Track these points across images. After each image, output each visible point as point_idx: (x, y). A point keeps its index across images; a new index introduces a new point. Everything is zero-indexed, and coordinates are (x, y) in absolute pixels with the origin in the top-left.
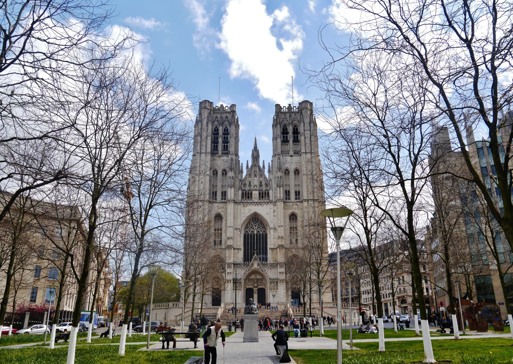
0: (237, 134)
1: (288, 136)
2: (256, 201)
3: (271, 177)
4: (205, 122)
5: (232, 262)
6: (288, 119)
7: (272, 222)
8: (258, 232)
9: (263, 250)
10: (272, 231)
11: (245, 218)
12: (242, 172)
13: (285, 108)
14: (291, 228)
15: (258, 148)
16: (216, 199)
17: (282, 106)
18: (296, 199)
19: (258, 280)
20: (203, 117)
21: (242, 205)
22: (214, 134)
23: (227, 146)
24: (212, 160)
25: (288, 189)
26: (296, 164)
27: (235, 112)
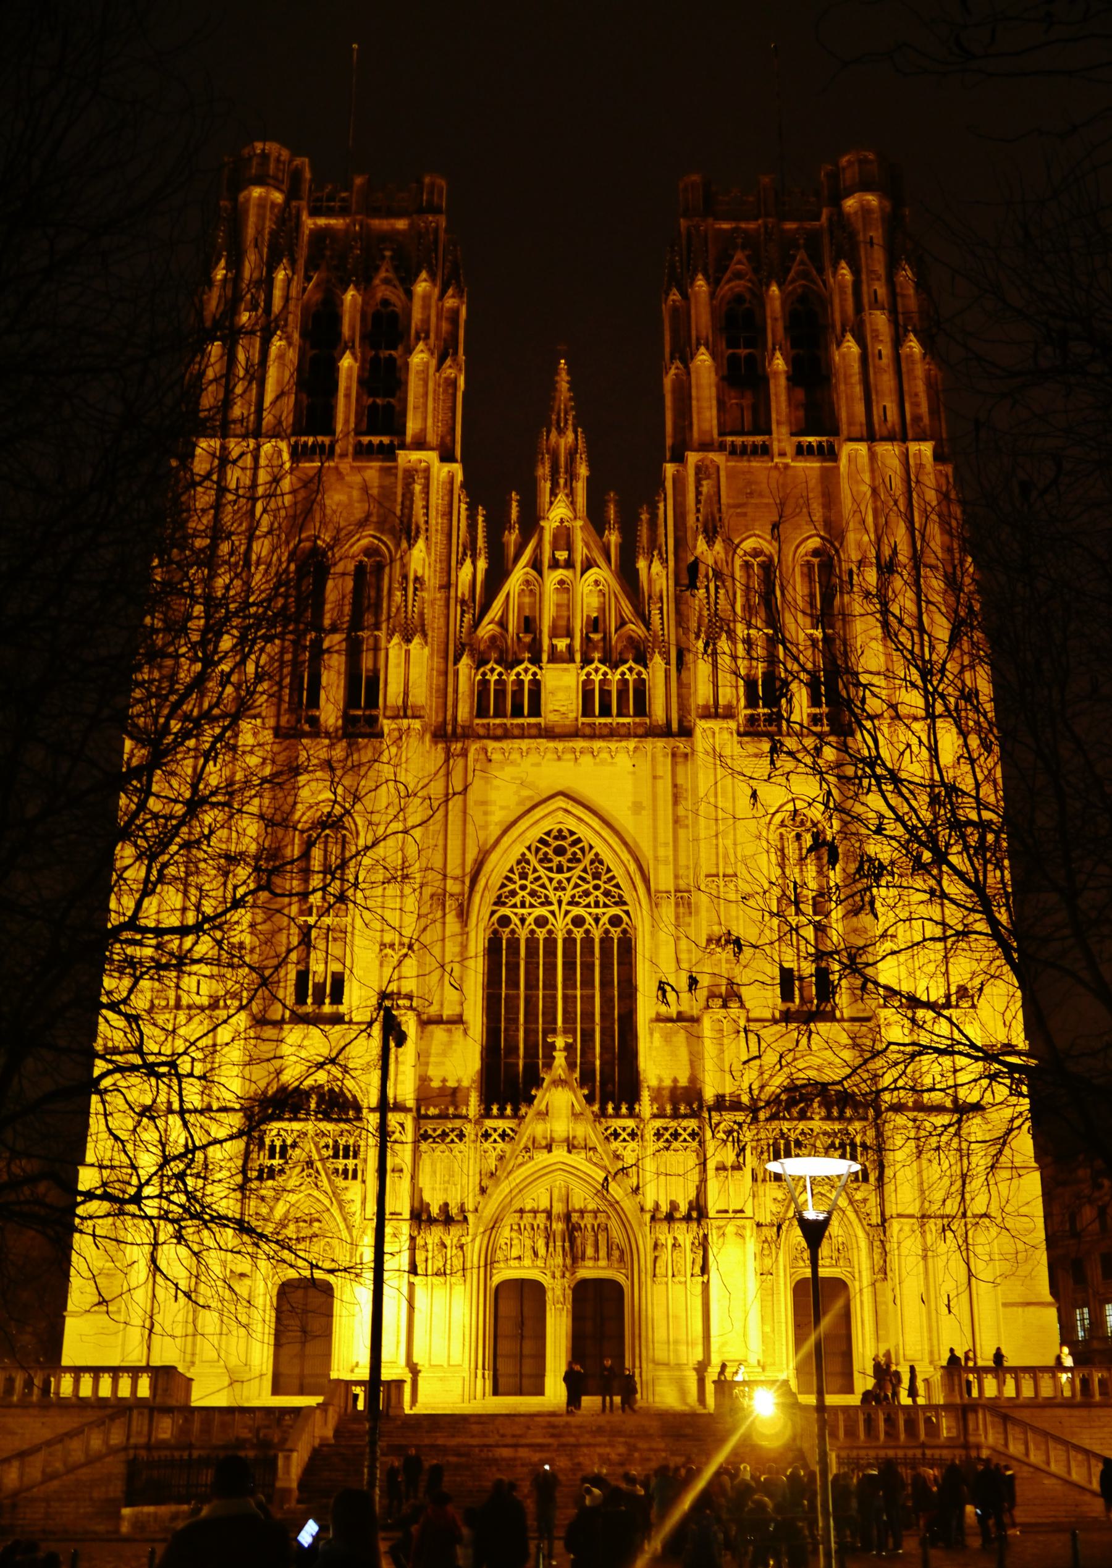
8: (578, 921)
16: (314, 721)
18: (815, 719)
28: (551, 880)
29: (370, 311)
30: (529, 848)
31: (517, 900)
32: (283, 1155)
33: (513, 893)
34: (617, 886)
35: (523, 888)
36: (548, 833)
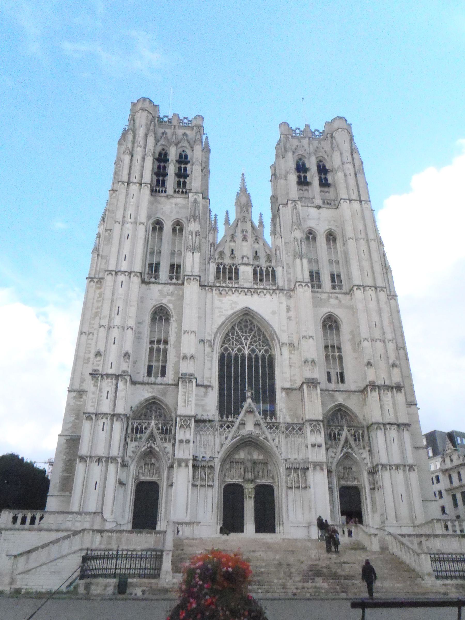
1: (308, 175)
3: (280, 242)
4: (141, 132)
5: (193, 413)
7: (284, 331)
8: (253, 351)
9: (264, 392)
10: (285, 351)
14: (326, 347)
15: (249, 190)
18: (334, 287)
19: (255, 463)
21: (215, 291)
23: (185, 183)
24: (151, 203)
25: (314, 269)
26: (329, 222)
28: (243, 336)
30: (235, 325)
31: (231, 342)
32: (141, 432)
33: (229, 340)
34: (267, 339)
35: (233, 338)
36: (242, 320)
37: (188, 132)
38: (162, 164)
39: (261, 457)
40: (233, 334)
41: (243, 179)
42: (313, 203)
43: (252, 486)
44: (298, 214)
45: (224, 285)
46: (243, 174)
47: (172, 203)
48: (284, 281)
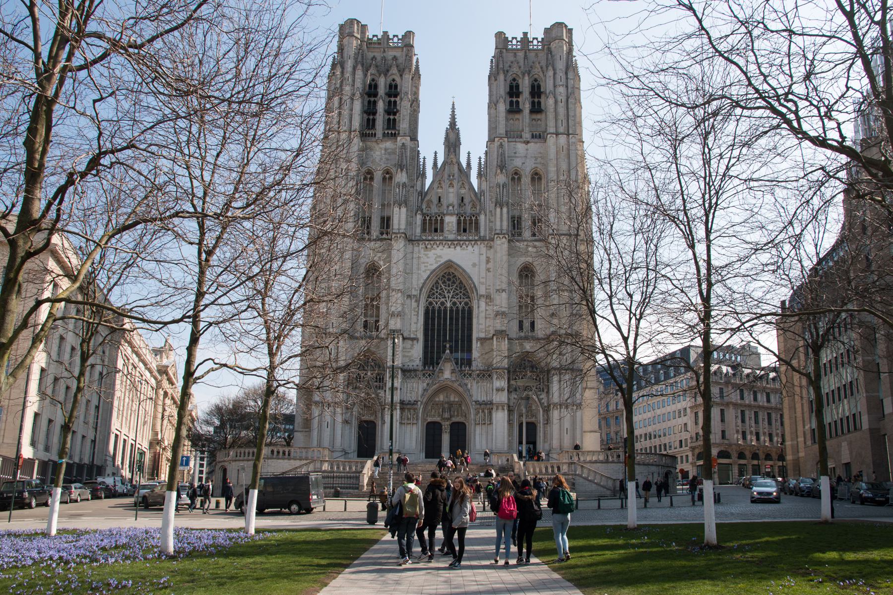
0: (416, 94)
1: (520, 100)
2: (451, 237)
3: (484, 187)
6: (522, 63)
7: (482, 284)
8: (454, 303)
9: (463, 341)
10: (483, 304)
11: (428, 273)
12: (423, 175)
13: (514, 42)
15: (459, 125)
17: (509, 36)
19: (451, 404)
20: (345, 55)
22: (369, 95)
23: (394, 120)
25: (516, 213)
27: (412, 46)
29: (388, 83)
37: (398, 54)
38: (372, 99)
39: (457, 400)
40: (437, 288)
41: (453, 112)
42: (521, 137)
43: (448, 423)
44: (503, 154)
45: (430, 238)
46: (453, 104)
47: (381, 148)
48: (485, 230)
